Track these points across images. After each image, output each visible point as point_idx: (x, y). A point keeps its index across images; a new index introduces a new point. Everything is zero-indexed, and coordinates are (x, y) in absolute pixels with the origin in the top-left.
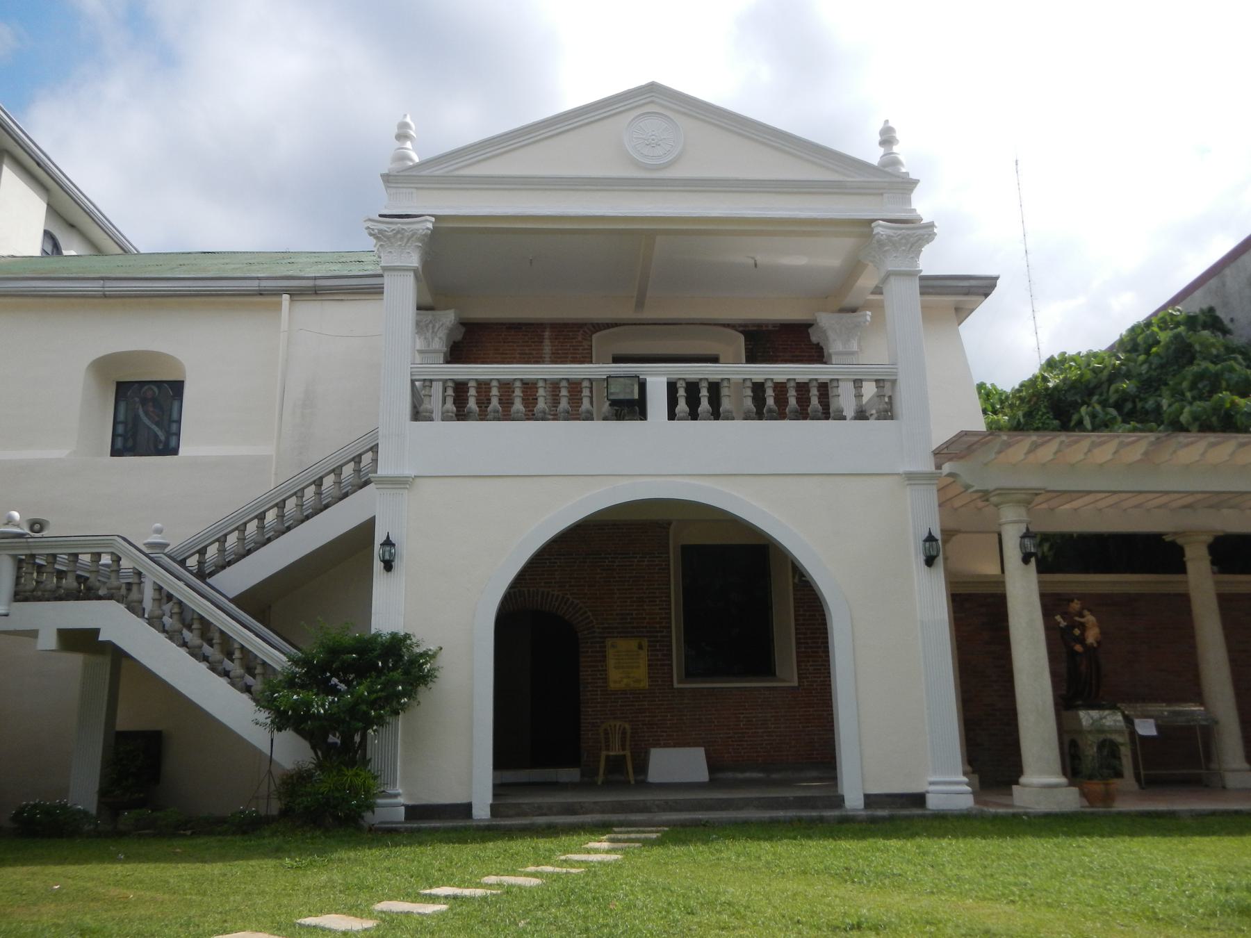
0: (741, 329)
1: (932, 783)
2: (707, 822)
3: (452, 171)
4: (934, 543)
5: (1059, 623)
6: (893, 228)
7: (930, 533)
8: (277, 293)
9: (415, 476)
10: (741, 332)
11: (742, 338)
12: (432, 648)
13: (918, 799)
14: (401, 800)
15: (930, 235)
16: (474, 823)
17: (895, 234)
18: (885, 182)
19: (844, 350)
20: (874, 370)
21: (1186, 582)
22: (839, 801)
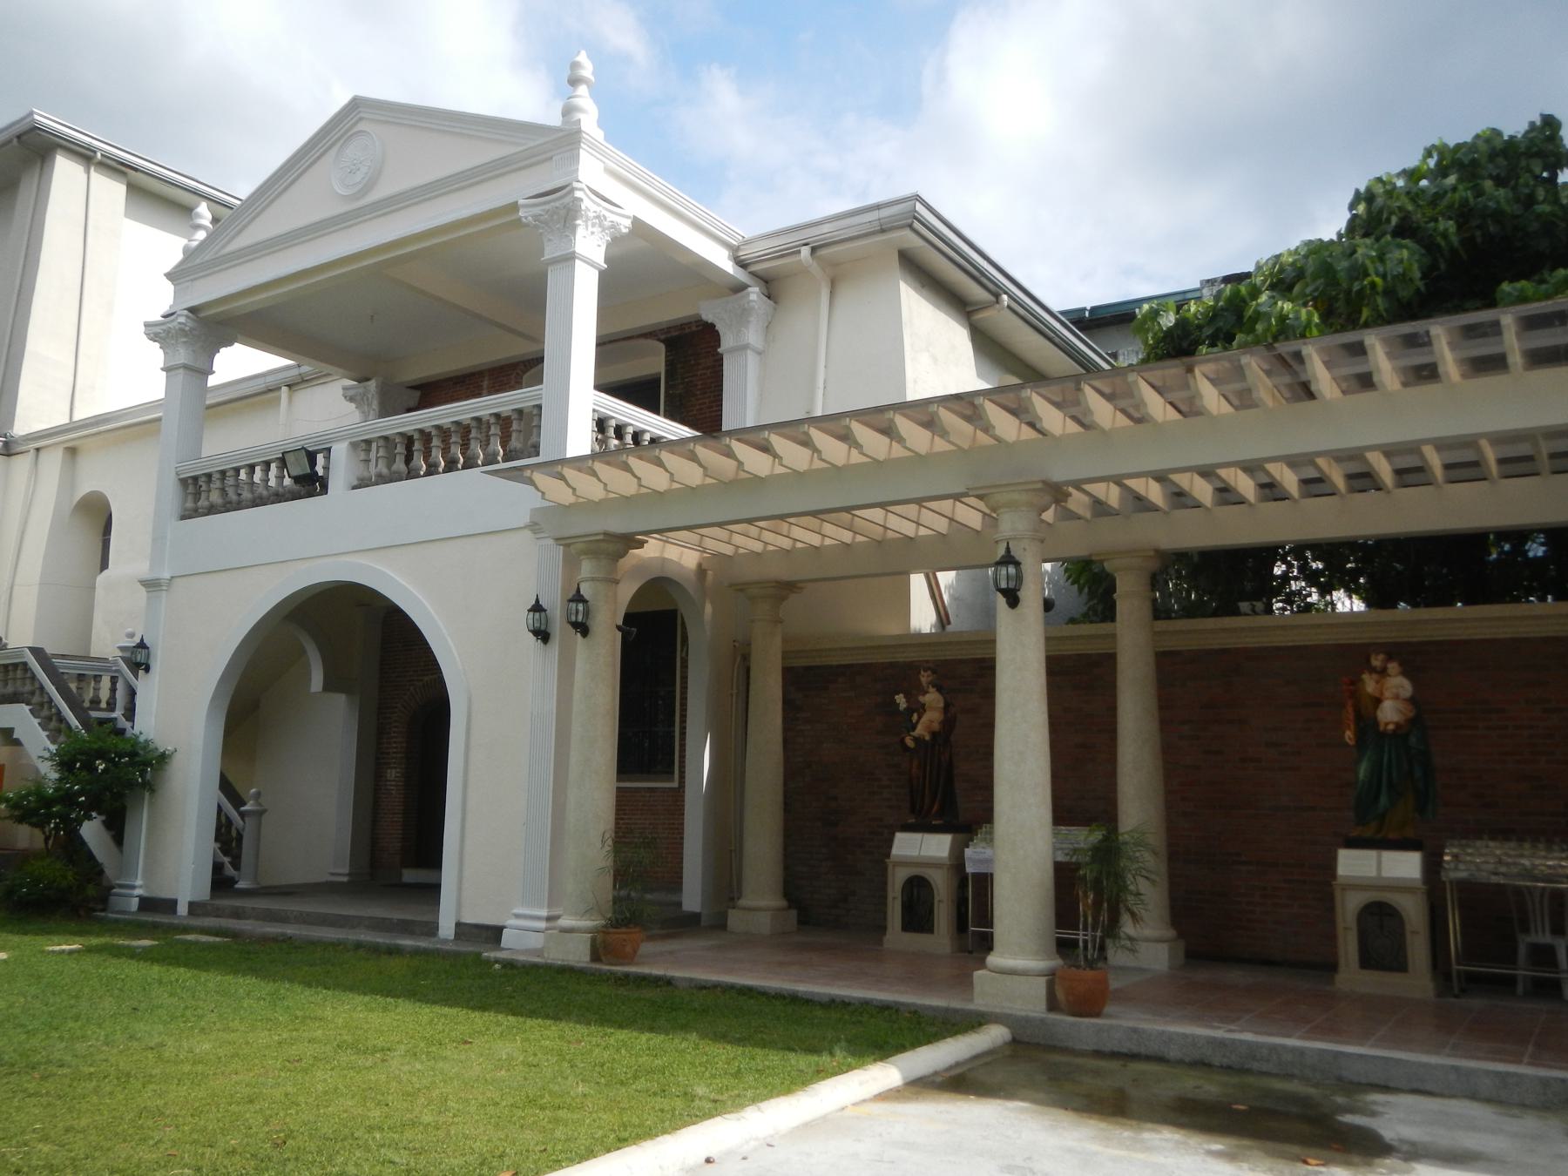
0: (663, 337)
1: (517, 916)
2: (291, 938)
3: (219, 250)
4: (543, 614)
6: (545, 203)
7: (537, 601)
9: (172, 577)
10: (662, 341)
11: (662, 347)
12: (169, 748)
13: (494, 934)
14: (138, 892)
15: (573, 202)
16: (176, 921)
17: (543, 210)
19: (735, 344)
21: (1113, 636)
22: (431, 929)
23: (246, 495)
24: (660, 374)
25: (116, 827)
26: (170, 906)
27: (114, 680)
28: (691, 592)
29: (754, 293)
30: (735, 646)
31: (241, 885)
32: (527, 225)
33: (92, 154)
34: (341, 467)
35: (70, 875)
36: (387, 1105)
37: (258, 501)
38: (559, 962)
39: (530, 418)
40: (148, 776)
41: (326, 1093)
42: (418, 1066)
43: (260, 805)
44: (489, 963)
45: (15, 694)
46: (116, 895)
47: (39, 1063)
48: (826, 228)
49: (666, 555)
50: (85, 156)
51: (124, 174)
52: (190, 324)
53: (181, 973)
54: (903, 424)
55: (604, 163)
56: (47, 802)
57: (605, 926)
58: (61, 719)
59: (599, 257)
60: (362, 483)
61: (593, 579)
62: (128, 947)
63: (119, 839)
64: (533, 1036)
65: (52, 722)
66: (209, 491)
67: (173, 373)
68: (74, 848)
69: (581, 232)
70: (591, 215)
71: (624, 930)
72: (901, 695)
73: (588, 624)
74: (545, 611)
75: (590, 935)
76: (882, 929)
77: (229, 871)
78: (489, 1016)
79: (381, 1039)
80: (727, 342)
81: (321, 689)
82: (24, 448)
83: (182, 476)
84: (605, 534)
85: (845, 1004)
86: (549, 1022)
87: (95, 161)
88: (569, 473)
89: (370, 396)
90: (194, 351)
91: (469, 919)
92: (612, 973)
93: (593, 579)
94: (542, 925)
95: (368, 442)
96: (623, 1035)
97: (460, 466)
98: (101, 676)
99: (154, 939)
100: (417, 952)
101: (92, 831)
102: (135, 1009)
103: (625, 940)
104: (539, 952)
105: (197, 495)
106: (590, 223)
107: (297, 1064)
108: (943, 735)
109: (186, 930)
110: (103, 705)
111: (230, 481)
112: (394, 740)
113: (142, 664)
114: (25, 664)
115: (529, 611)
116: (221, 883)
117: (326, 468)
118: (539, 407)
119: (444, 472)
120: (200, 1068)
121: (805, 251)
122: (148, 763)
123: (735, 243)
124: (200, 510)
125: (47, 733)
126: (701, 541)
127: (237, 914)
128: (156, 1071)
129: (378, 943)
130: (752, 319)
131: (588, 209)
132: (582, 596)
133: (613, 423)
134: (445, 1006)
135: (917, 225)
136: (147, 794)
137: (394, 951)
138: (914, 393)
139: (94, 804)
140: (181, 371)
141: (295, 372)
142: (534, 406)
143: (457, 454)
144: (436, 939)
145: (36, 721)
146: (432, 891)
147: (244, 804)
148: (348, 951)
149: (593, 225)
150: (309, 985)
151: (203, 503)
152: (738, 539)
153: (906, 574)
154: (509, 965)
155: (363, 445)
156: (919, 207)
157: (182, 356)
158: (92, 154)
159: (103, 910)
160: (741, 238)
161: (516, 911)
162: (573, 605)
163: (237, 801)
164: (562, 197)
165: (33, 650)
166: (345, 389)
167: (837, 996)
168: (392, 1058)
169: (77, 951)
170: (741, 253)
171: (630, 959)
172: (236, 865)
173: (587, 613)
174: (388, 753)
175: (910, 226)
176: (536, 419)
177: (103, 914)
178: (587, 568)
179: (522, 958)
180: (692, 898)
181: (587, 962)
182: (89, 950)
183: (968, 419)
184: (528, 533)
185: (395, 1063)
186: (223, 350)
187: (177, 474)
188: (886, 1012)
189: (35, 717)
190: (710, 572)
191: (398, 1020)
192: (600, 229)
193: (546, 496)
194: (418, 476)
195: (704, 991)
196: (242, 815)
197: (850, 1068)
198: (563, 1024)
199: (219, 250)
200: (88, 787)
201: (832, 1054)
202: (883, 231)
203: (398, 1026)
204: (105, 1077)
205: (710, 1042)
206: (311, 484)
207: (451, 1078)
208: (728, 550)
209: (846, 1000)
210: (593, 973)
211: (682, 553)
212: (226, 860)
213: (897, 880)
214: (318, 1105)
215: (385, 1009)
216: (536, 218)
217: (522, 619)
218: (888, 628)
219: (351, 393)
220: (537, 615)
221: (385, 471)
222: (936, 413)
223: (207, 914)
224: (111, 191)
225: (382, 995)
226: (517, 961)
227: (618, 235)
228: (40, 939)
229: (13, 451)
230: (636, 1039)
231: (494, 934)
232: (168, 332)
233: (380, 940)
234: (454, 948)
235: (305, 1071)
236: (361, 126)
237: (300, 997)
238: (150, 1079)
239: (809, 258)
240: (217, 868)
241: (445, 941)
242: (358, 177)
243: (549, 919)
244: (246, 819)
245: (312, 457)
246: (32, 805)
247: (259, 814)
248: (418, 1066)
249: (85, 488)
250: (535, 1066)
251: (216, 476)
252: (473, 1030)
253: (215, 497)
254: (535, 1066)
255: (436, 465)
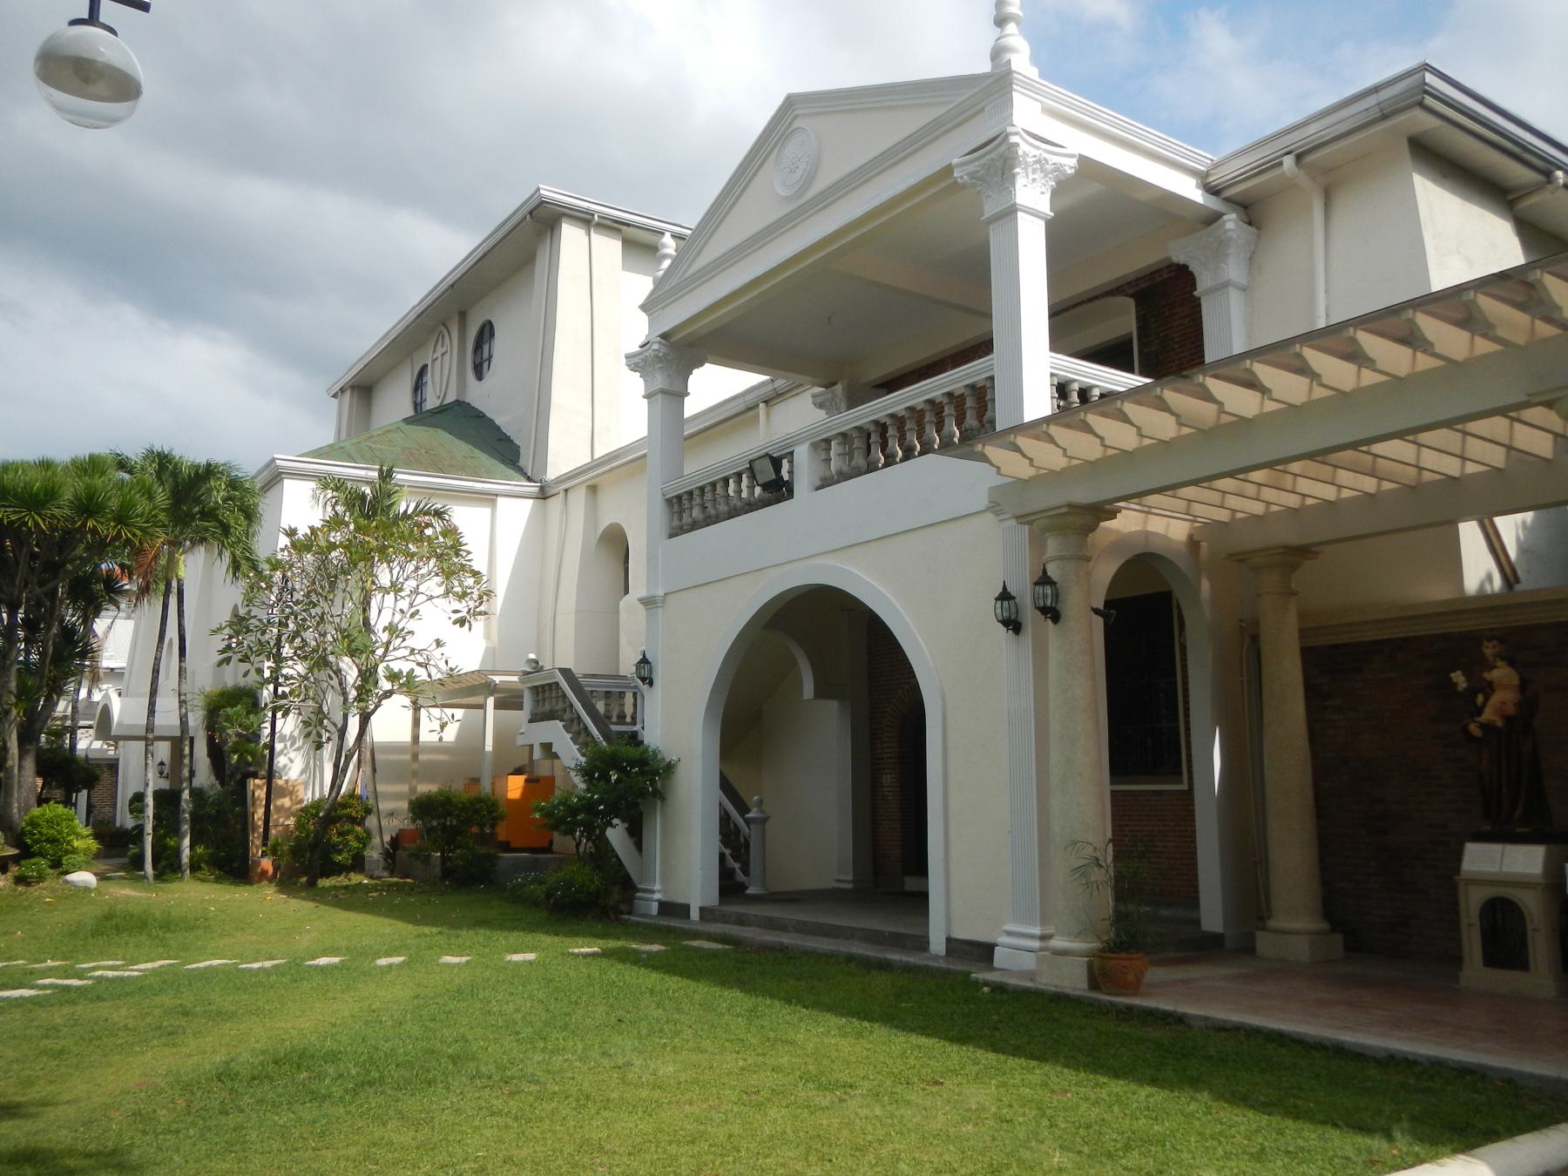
0: (1131, 291)
1: (1009, 933)
2: (787, 948)
3: (683, 275)
4: (1012, 602)
5: (1456, 684)
8: (753, 407)
10: (1131, 296)
11: (1131, 303)
13: (985, 952)
14: (657, 896)
16: (686, 927)
18: (976, 93)
20: (958, 375)
22: (922, 944)
23: (723, 508)
24: (1131, 333)
25: (636, 832)
26: (681, 910)
27: (635, 694)
28: (1182, 565)
29: (1231, 221)
30: (1241, 627)
31: (751, 891)
32: (964, 186)
33: (590, 217)
34: (804, 468)
35: (596, 879)
36: (830, 1161)
37: (733, 512)
38: (1053, 989)
39: (982, 395)
40: (659, 786)
41: (771, 1137)
42: (878, 1111)
43: (762, 812)
44: (978, 985)
45: (551, 711)
46: (640, 899)
47: (512, 1078)
48: (1312, 129)
49: (1150, 528)
50: (586, 220)
51: (619, 230)
52: (664, 350)
53: (674, 983)
54: (1429, 326)
55: (1041, 102)
56: (573, 811)
57: (1102, 950)
58: (589, 734)
59: (1044, 205)
60: (825, 483)
61: (1060, 558)
62: (636, 952)
63: (639, 846)
64: (1012, 1081)
65: (580, 734)
66: (691, 508)
67: (654, 398)
68: (603, 855)
69: (1020, 182)
70: (1030, 160)
71: (1123, 955)
72: (1459, 673)
73: (1058, 608)
74: (1014, 598)
75: (1086, 959)
76: (1455, 960)
77: (740, 876)
78: (967, 1051)
79: (847, 1071)
80: (1204, 283)
81: (812, 697)
82: (554, 491)
83: (667, 497)
84: (1070, 506)
85: (1407, 1063)
86: (1034, 1063)
87: (594, 223)
88: (1022, 441)
89: (838, 400)
90: (669, 376)
91: (960, 934)
92: (1111, 1004)
93: (1060, 558)
94: (1036, 944)
95: (828, 441)
96: (1118, 1087)
97: (916, 453)
98: (624, 693)
99: (663, 944)
100: (908, 968)
101: (616, 835)
102: (620, 1020)
103: (1125, 967)
104: (1031, 975)
105: (681, 513)
106: (1030, 170)
107: (754, 1097)
108: (1521, 721)
109: (696, 935)
110: (628, 719)
111: (708, 496)
112: (887, 745)
113: (646, 679)
114: (557, 684)
115: (997, 599)
116: (730, 887)
117: (791, 472)
118: (992, 378)
119: (902, 460)
120: (657, 1094)
121: (1288, 161)
122: (657, 773)
123: (1202, 168)
124: (685, 527)
125: (577, 747)
126: (1189, 508)
127: (741, 921)
128: (615, 1095)
129: (869, 956)
130: (1231, 251)
131: (1025, 154)
132: (1049, 577)
133: (1076, 386)
134: (922, 1034)
135: (1429, 101)
136: (659, 803)
137: (885, 966)
138: (1440, 281)
139: (614, 810)
140: (659, 396)
141: (770, 387)
142: (987, 378)
143: (913, 441)
144: (926, 954)
145: (568, 736)
146: (920, 900)
147: (749, 811)
148: (840, 964)
149: (1034, 171)
150: (789, 1002)
151: (686, 519)
152: (1233, 502)
153: (1452, 524)
154: (999, 988)
155: (823, 444)
156: (1429, 78)
157: (660, 381)
158: (590, 217)
159: (630, 913)
160: (1209, 162)
161: (1008, 927)
162: (1039, 589)
163: (743, 808)
164: (996, 147)
165: (560, 670)
166: (814, 396)
167: (1398, 1051)
168: (852, 1097)
169: (594, 955)
170: (1211, 180)
171: (1134, 988)
172: (746, 872)
173: (1056, 596)
174: (882, 759)
175: (1421, 104)
176: (989, 392)
177: (627, 917)
178: (1053, 546)
179: (1013, 981)
180: (1212, 915)
181: (1084, 990)
182: (605, 954)
183: (1521, 307)
184: (990, 516)
185: (853, 1104)
186: (695, 371)
187: (664, 495)
188: (1468, 1078)
189: (568, 732)
190: (1203, 544)
191: (869, 1050)
192: (1042, 175)
193: (1002, 472)
194: (877, 469)
195: (1224, 1034)
196: (748, 822)
197: (1419, 1161)
198: (1047, 1067)
199: (683, 275)
200: (606, 796)
201: (1389, 1137)
202: (1384, 117)
203: (868, 1057)
204: (567, 1098)
205: (1226, 1105)
206: (779, 490)
207: (909, 1130)
208: (1223, 516)
209: (1410, 1057)
210: (1091, 1003)
211: (1168, 524)
212: (737, 866)
213: (1472, 902)
214: (758, 1153)
215: (859, 1035)
216: (972, 175)
217: (987, 610)
218: (1435, 592)
219: (819, 400)
220: (1006, 603)
221: (845, 469)
222: (1474, 302)
223: (715, 920)
224: (609, 248)
225: (859, 1018)
226: (1008, 984)
227: (1062, 178)
228: (568, 940)
229: (548, 495)
230: (1134, 1094)
231: (985, 952)
232: (645, 360)
233: (869, 953)
234: (944, 966)
235: (760, 1105)
236: (796, 124)
237: (778, 1014)
238: (607, 1104)
239: (1295, 169)
240: (725, 875)
241: (937, 957)
242: (799, 172)
243: (1043, 938)
244: (752, 826)
245: (776, 463)
246: (561, 814)
247: (763, 821)
248: (878, 1111)
249: (605, 521)
250: (1007, 1122)
251: (696, 493)
252: (947, 1067)
253: (696, 513)
254: (1007, 1122)
255: (894, 456)
